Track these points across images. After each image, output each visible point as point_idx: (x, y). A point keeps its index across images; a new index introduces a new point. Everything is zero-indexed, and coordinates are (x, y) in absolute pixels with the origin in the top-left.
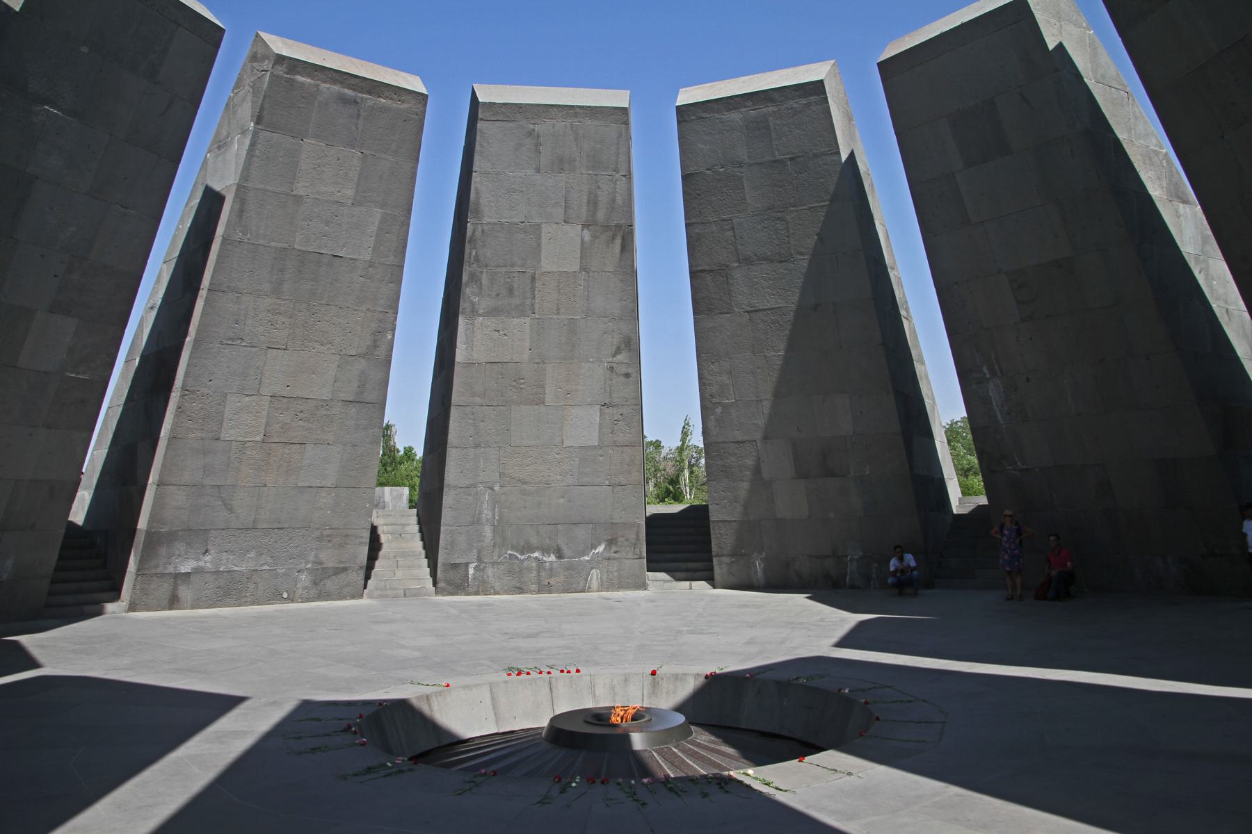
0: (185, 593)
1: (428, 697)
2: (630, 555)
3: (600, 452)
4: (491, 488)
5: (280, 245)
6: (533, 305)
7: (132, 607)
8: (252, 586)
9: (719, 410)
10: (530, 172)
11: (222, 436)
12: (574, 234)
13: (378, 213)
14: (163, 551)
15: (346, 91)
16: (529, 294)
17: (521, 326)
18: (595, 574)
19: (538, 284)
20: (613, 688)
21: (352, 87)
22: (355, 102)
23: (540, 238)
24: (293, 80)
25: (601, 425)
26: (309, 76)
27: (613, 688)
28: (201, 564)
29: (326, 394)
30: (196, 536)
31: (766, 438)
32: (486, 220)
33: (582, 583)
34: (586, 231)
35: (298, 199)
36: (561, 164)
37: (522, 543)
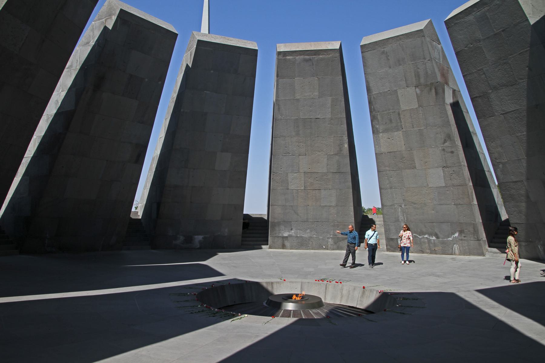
0: (287, 244)
1: (272, 283)
2: (472, 239)
3: (447, 189)
4: (401, 206)
6: (401, 125)
7: (270, 248)
8: (311, 243)
9: (501, 166)
11: (289, 188)
12: (412, 91)
13: (330, 99)
14: (277, 229)
15: (306, 57)
16: (399, 121)
18: (456, 246)
19: (402, 116)
20: (349, 291)
21: (308, 55)
22: (310, 60)
23: (398, 96)
25: (444, 176)
27: (349, 291)
28: (291, 233)
29: (325, 170)
30: (288, 224)
31: (528, 179)
32: (374, 93)
33: (451, 251)
34: (417, 89)
35: (298, 100)
36: (399, 62)
37: (419, 231)
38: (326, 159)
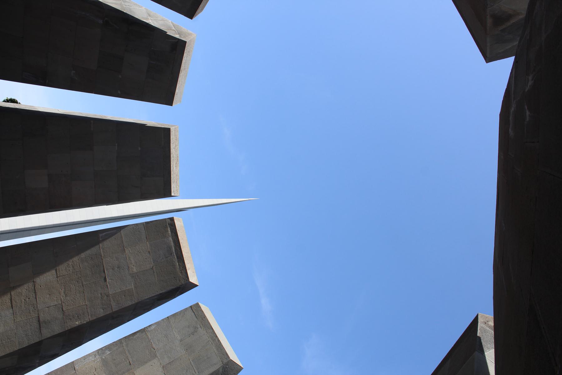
5: (102, 253)
10: (179, 338)
15: (173, 248)
21: (176, 250)
26: (171, 232)
38: (56, 303)
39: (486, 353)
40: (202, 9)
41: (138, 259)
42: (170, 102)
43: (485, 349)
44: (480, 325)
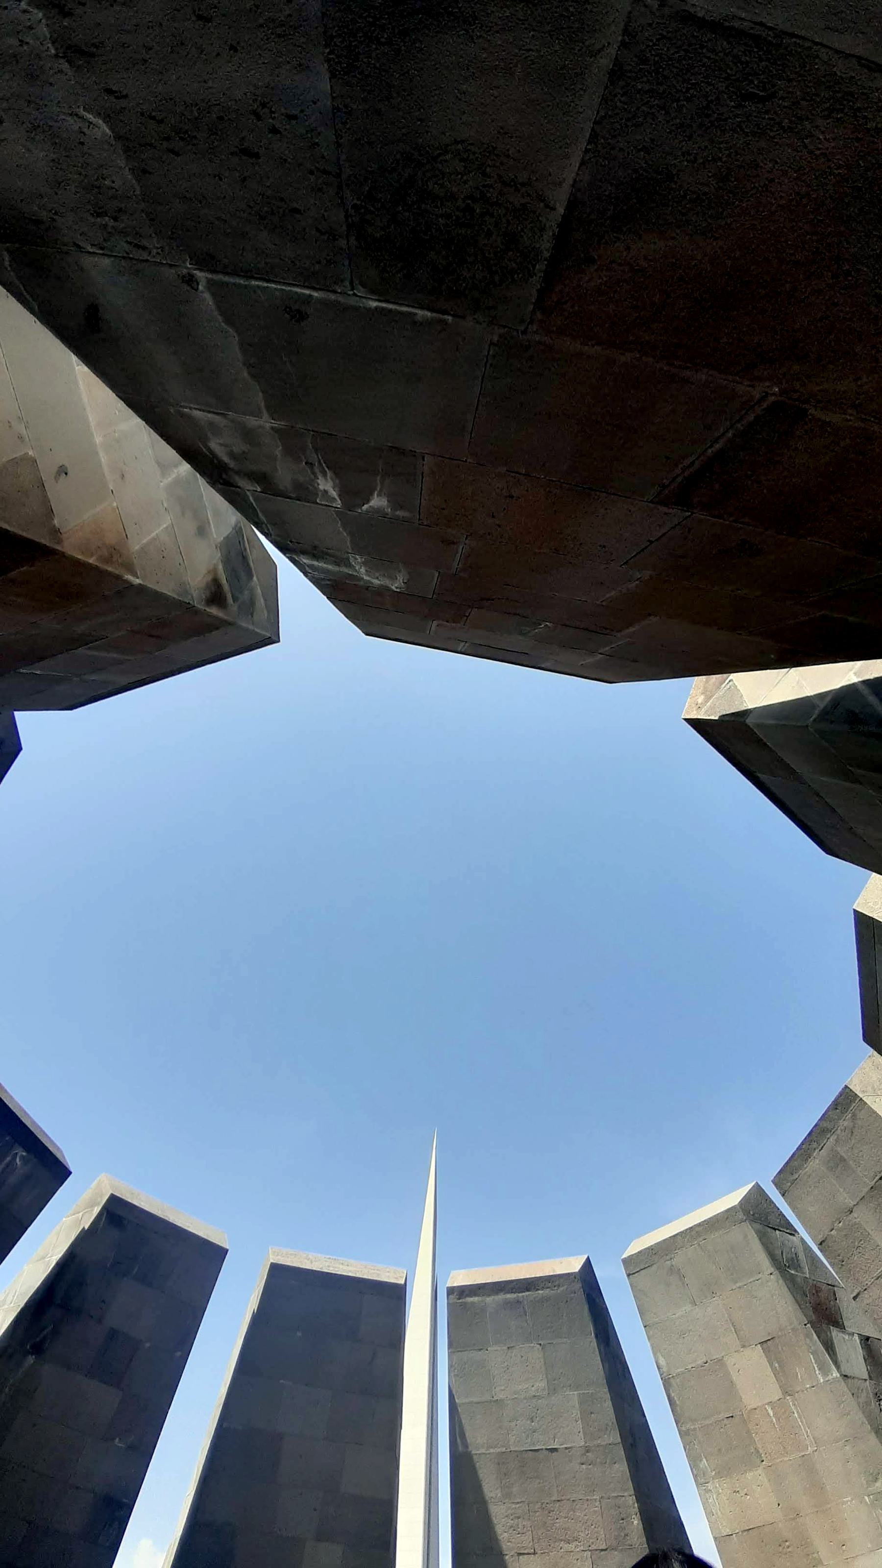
5: (499, 1450)
10: (688, 1307)
15: (509, 1296)
17: (756, 1479)
24: (465, 1303)
36: (710, 1289)
39: (750, 707)
40: (58, 1149)
41: (519, 1372)
42: (221, 1253)
43: (743, 708)
44: (702, 716)
